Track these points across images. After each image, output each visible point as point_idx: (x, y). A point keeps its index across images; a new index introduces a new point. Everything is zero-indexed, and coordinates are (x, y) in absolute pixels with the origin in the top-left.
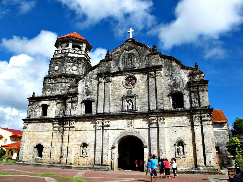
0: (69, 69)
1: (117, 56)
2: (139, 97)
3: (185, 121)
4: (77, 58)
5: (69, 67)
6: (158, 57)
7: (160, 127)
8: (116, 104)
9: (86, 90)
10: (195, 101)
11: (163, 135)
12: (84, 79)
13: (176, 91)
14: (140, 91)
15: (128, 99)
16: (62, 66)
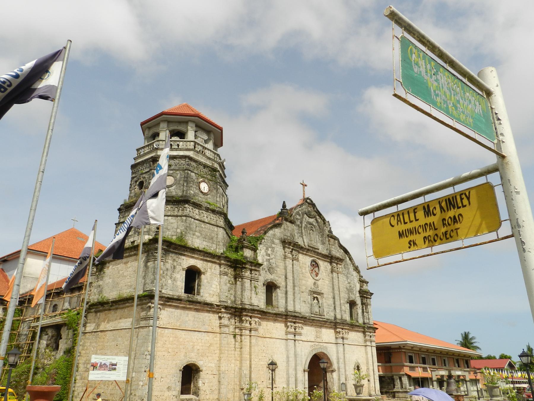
1: (299, 219)
15: (315, 296)
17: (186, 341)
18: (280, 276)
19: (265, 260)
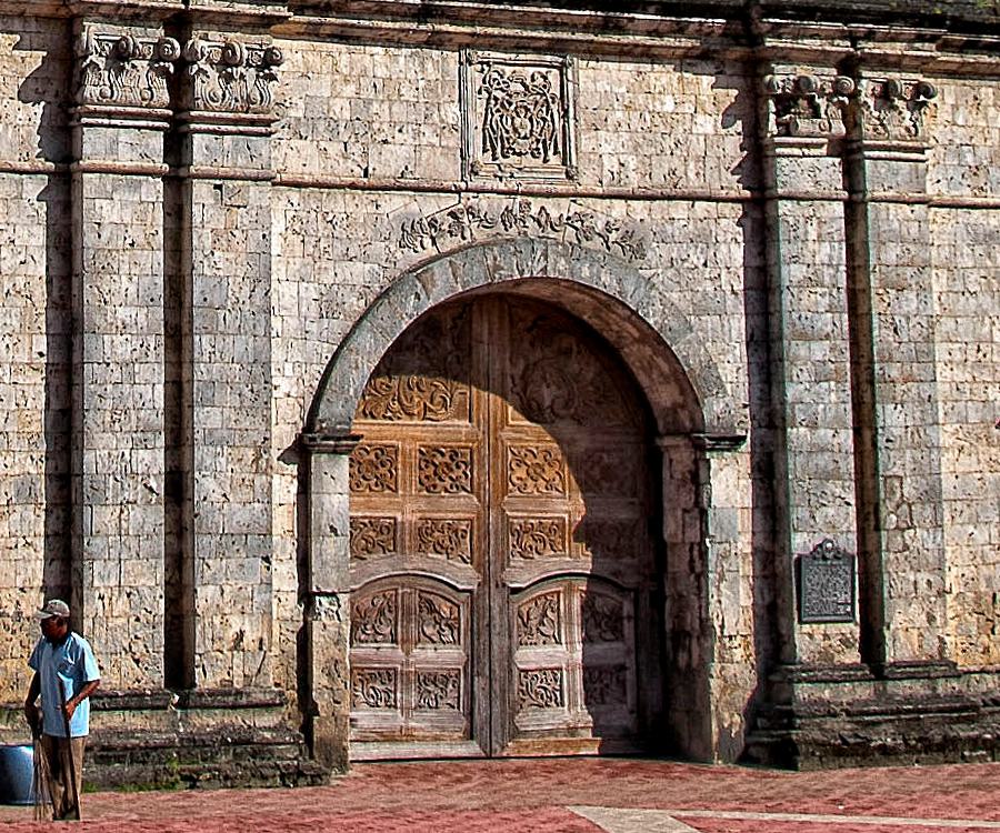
7: (880, 194)
11: (910, 301)
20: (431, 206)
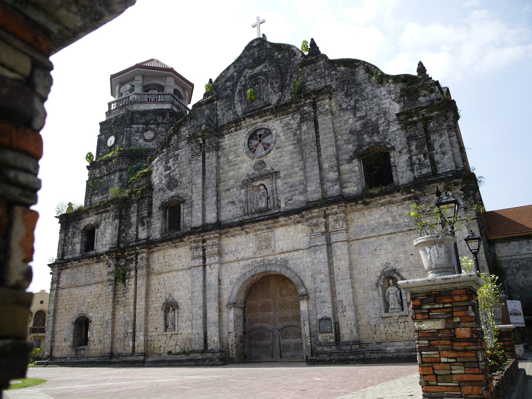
0: (138, 140)
1: (229, 87)
2: (282, 175)
3: (397, 218)
4: (155, 112)
5: (137, 134)
6: (321, 69)
8: (231, 200)
9: (167, 179)
10: (420, 160)
12: (162, 154)
13: (370, 143)
14: (282, 158)
15: (258, 183)
16: (121, 134)
17: (78, 296)
18: (186, 186)
19: (163, 178)
20: (249, 262)
